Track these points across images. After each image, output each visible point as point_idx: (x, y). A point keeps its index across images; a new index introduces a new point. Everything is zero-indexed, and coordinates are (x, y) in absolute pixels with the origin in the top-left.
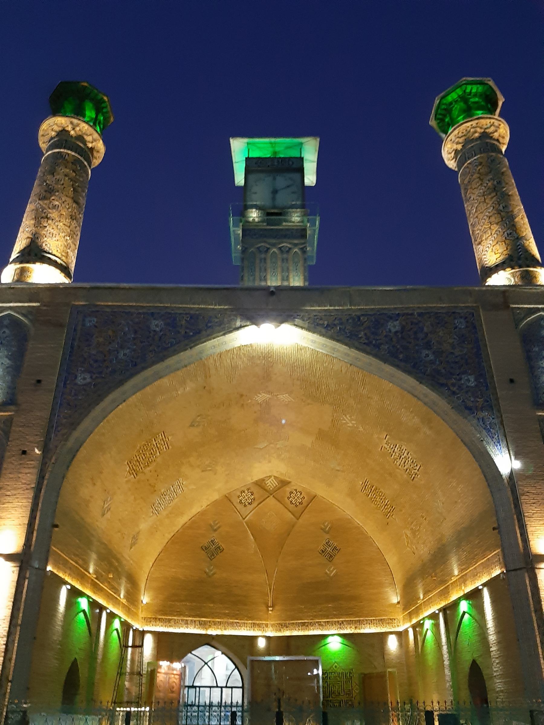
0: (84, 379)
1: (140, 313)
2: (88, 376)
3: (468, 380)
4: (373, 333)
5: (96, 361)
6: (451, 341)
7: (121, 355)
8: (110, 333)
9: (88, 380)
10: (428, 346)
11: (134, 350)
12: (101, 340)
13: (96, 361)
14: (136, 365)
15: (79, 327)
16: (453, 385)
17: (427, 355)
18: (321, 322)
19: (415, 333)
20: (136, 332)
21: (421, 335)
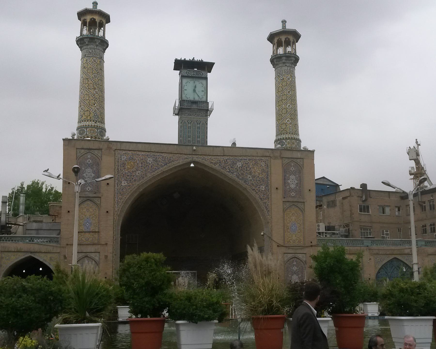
0: (125, 183)
1: (142, 155)
2: (126, 182)
3: (262, 188)
4: (231, 167)
5: (128, 176)
6: (258, 171)
7: (137, 174)
8: (132, 163)
9: (126, 184)
10: (250, 173)
11: (142, 171)
12: (129, 166)
13: (128, 176)
14: (143, 178)
15: (119, 161)
16: (257, 190)
17: (250, 177)
18: (212, 161)
19: (247, 168)
20: (142, 163)
21: (248, 169)
